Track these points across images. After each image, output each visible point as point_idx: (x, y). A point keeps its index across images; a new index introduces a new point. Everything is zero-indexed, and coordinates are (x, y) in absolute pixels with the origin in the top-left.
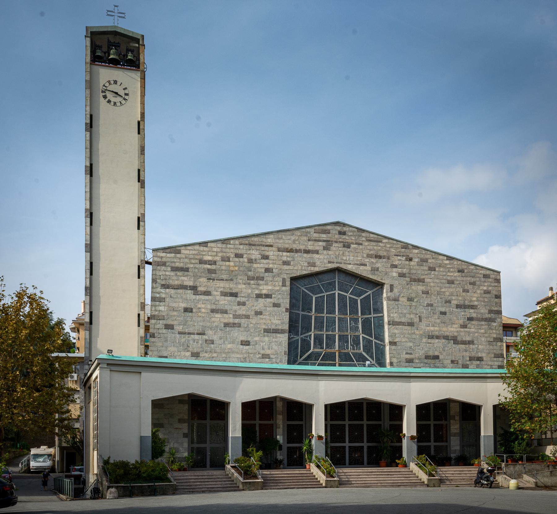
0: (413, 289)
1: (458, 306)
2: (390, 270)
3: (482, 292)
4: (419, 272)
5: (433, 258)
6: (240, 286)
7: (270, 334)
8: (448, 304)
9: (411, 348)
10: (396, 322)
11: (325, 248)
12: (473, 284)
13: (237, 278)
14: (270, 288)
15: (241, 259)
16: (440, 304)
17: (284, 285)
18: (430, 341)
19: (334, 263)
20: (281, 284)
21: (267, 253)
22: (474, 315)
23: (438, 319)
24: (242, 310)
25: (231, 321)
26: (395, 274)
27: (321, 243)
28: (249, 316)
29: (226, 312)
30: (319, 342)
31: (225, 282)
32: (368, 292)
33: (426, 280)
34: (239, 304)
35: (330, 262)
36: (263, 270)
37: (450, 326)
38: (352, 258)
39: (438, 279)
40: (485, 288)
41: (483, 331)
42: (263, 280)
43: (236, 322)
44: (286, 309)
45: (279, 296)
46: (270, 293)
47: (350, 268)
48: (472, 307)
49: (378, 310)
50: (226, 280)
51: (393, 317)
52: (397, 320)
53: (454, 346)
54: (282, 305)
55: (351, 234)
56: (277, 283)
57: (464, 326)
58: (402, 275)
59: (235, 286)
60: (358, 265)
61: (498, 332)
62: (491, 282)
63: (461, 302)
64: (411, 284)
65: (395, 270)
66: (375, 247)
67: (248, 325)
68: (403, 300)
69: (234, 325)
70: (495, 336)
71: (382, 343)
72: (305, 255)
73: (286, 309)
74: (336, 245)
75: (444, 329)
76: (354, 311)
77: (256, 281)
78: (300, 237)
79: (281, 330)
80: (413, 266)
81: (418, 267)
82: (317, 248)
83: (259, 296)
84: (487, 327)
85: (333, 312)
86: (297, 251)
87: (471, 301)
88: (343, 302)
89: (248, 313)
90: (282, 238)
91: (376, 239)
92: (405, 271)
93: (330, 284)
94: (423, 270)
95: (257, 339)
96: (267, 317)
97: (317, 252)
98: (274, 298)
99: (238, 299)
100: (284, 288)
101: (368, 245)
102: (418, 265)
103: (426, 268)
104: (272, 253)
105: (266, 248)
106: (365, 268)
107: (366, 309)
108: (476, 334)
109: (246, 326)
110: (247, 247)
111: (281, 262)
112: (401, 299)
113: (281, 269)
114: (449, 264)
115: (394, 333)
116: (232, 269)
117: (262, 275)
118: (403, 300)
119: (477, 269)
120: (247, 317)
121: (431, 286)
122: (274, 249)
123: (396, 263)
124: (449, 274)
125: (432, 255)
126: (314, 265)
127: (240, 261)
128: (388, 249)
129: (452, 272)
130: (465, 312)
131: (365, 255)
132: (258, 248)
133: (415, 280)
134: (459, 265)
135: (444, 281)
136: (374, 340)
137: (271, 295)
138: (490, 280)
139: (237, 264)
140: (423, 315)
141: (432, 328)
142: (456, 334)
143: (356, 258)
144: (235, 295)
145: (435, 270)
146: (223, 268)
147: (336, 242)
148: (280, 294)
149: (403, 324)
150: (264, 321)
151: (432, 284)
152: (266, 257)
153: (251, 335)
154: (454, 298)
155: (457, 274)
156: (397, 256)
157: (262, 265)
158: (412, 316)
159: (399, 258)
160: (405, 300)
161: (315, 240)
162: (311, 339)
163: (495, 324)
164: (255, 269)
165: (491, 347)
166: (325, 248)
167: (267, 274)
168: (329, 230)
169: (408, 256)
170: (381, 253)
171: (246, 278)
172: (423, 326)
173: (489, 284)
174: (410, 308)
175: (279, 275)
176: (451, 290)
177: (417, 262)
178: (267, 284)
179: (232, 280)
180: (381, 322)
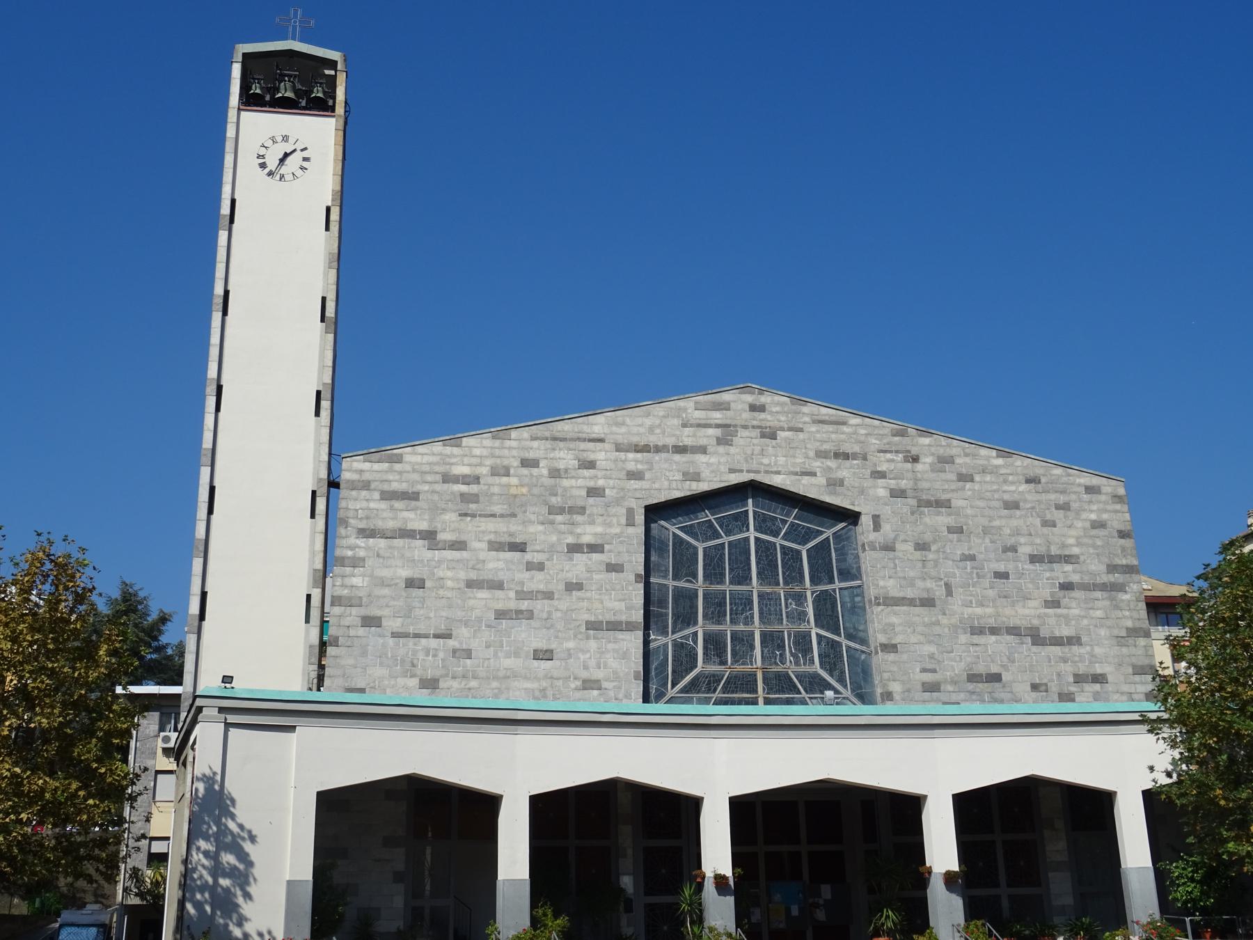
1: (1034, 559)
3: (1088, 525)
4: (938, 485)
5: (966, 455)
6: (532, 529)
8: (1009, 554)
9: (931, 656)
11: (720, 441)
12: (1065, 507)
13: (525, 512)
14: (599, 529)
15: (535, 471)
16: (992, 556)
17: (630, 523)
18: (976, 639)
19: (742, 471)
20: (623, 521)
21: (592, 457)
22: (1075, 578)
24: (537, 581)
25: (512, 605)
26: (882, 492)
27: (711, 431)
29: (499, 586)
30: (716, 649)
32: (822, 533)
33: (954, 503)
34: (530, 566)
35: (732, 471)
36: (584, 493)
38: (782, 460)
40: (1093, 516)
41: (1099, 613)
44: (638, 576)
46: (599, 542)
47: (777, 481)
48: (1068, 559)
49: (849, 573)
50: (502, 516)
53: (1034, 649)
55: (778, 409)
56: (615, 520)
57: (1054, 604)
58: (897, 494)
59: (520, 528)
60: (796, 474)
61: (1135, 615)
62: (1105, 503)
64: (922, 513)
65: (881, 482)
66: (833, 436)
67: (549, 613)
68: (905, 548)
70: (1129, 624)
71: (864, 648)
72: (677, 457)
73: (638, 576)
74: (746, 433)
75: (1008, 611)
76: (794, 575)
77: (568, 517)
79: (628, 623)
81: (933, 475)
82: (703, 442)
83: (575, 548)
84: (1107, 603)
85: (746, 579)
86: (658, 449)
87: (1064, 546)
88: (767, 556)
89: (551, 587)
90: (623, 424)
91: (833, 419)
92: (904, 484)
93: (736, 517)
94: (947, 481)
95: (571, 644)
96: (594, 595)
97: (703, 450)
98: (610, 551)
99: (528, 556)
100: (631, 530)
101: (818, 431)
104: (601, 455)
105: (591, 445)
106: (813, 480)
107: (821, 571)
108: (1085, 622)
109: (545, 615)
110: (548, 444)
111: (623, 475)
113: (623, 489)
116: (513, 491)
117: (580, 503)
118: (904, 548)
119: (1069, 475)
120: (549, 595)
121: (967, 516)
122: (606, 446)
123: (883, 467)
124: (1006, 488)
125: (964, 449)
126: (696, 477)
127: (531, 475)
128: (862, 438)
129: (1013, 483)
131: (812, 454)
132: (572, 445)
133: (929, 504)
136: (845, 643)
137: (602, 546)
138: (1103, 498)
139: (526, 480)
141: (979, 611)
142: (1036, 622)
143: (792, 460)
144: (519, 547)
145: (972, 480)
146: (496, 490)
147: (745, 427)
148: (621, 542)
149: (911, 602)
150: (585, 604)
151: (969, 511)
152: (591, 465)
154: (1022, 540)
155: (1023, 487)
157: (580, 482)
158: (929, 584)
159: (889, 456)
160: (909, 547)
161: (699, 426)
162: (695, 642)
163: (1126, 597)
164: (565, 489)
165: (1125, 650)
166: (720, 441)
167: (591, 500)
168: (729, 403)
169: (909, 451)
170: (847, 448)
171: (545, 510)
173: (1101, 506)
174: (924, 567)
175: (618, 501)
176: (1014, 523)
177: (931, 465)
178: (592, 523)
179: (514, 515)
180: (857, 599)
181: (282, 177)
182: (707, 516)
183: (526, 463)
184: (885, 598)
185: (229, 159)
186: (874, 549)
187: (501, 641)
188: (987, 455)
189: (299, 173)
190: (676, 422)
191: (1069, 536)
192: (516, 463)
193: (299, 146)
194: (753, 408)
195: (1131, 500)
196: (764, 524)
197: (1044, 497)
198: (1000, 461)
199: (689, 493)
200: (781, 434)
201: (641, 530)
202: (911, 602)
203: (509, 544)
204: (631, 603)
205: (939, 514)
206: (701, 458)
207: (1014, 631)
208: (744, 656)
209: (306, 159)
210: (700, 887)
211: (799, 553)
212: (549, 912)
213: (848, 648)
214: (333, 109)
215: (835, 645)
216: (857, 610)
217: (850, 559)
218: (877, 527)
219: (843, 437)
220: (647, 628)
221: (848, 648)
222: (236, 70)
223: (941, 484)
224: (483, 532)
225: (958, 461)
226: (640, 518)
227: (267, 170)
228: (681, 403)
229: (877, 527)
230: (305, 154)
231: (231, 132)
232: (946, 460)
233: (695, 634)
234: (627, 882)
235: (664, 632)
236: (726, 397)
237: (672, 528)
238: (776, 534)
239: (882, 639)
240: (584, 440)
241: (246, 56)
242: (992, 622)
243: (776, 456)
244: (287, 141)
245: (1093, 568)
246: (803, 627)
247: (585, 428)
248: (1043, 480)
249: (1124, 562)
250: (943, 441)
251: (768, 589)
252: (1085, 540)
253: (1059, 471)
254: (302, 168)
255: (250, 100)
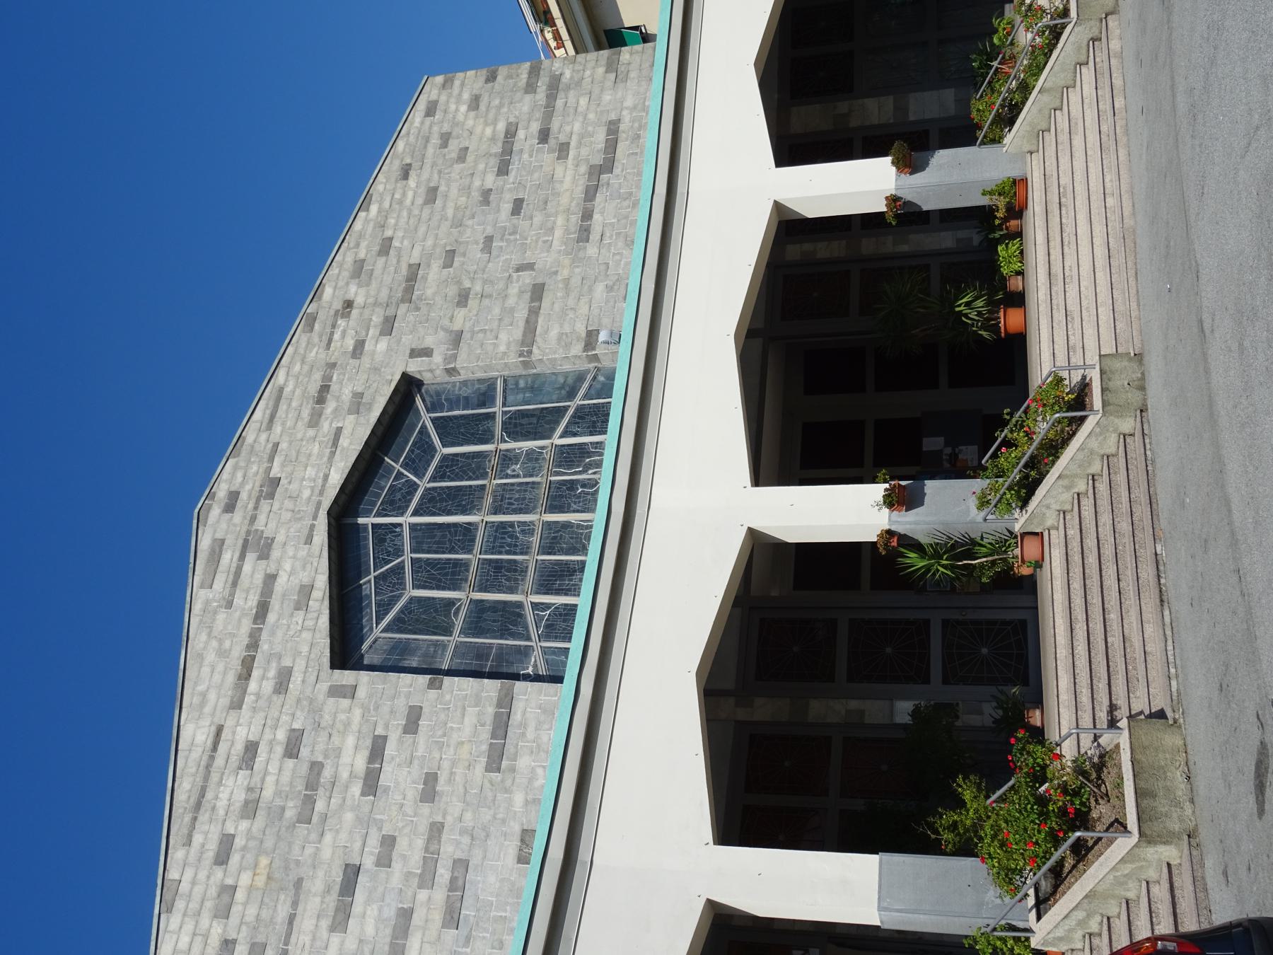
0: (435, 294)
1: (503, 170)
2: (366, 361)
3: (472, 114)
4: (388, 279)
5: (358, 245)
6: (326, 853)
7: (509, 749)
8: (492, 198)
9: (609, 289)
10: (525, 334)
11: (264, 555)
12: (445, 139)
13: (298, 863)
14: (350, 741)
15: (239, 842)
16: (490, 218)
17: (350, 692)
18: (595, 236)
19: (312, 526)
20: (345, 703)
21: (239, 747)
22: (535, 127)
23: (531, 218)
24: (410, 851)
25: (439, 895)
26: (383, 345)
27: (247, 568)
28: (433, 824)
29: (406, 915)
30: (561, 577)
31: (300, 908)
32: (424, 430)
33: (414, 260)
34: (384, 861)
35: (309, 540)
36: (290, 763)
37: (557, 186)
38: (310, 472)
39: (416, 229)
40: (463, 108)
41: (583, 101)
42: (321, 765)
43: (447, 876)
44: (431, 685)
45: (385, 709)
46: (369, 742)
47: (337, 478)
48: (510, 134)
49: (484, 394)
50: (295, 904)
51: (509, 344)
52: (518, 333)
53: (617, 171)
54: (414, 702)
55: (239, 475)
56: (342, 717)
57: (563, 149)
58: (388, 327)
59: (320, 873)
60: (333, 453)
61: (592, 64)
62: (450, 96)
63: (491, 164)
64: (420, 299)
65: (368, 346)
66: (294, 404)
67: (463, 832)
68: (461, 319)
69: (457, 886)
70: (601, 70)
71: (589, 377)
72: (271, 617)
73: (431, 685)
74: (262, 518)
75: (565, 200)
76: (474, 466)
77: (321, 791)
78: (215, 633)
79: (499, 705)
80: (367, 296)
81: (374, 285)
82: (259, 578)
83: (371, 783)
84: (572, 93)
85: (469, 529)
86: (254, 644)
87: (493, 139)
88: (442, 500)
89: (423, 827)
90: (204, 695)
91: (271, 403)
92: (377, 319)
93: (379, 541)
94: (385, 268)
95: (519, 798)
96: (449, 754)
97: (271, 579)
98: (387, 727)
99: (368, 862)
100: (361, 693)
101: (283, 424)
102: (368, 285)
103: (381, 261)
104: (240, 732)
105: (223, 747)
106: (346, 432)
107: (476, 429)
108: (591, 116)
109: (466, 840)
110: (203, 817)
111: (278, 700)
112: (457, 326)
113: (299, 701)
114: (381, 203)
115: (559, 339)
116: (261, 881)
117: (304, 769)
118: (461, 319)
119: (408, 134)
120: (436, 830)
121: (435, 245)
122: (229, 723)
123: (350, 343)
124: (408, 202)
125: (349, 248)
126: (306, 591)
127: (244, 848)
128: (306, 368)
129: (404, 194)
130: (522, 151)
131: (311, 432)
132: (215, 777)
133: (409, 290)
134: (388, 179)
135: (427, 211)
136: (578, 401)
137: (376, 738)
138: (443, 98)
139: (250, 857)
140: (516, 259)
141: (558, 233)
142: (583, 169)
143: (313, 458)
144: (352, 873)
145: (391, 239)
146: (252, 911)
147: (253, 519)
148: (377, 708)
149: (534, 312)
150: (459, 771)
151: (430, 242)
152: (251, 749)
153: (504, 821)
154: (477, 183)
155: (412, 182)
156: (330, 341)
157: (273, 769)
158: (514, 290)
159: (337, 336)
160: (461, 314)
161: (235, 584)
162: (548, 606)
163: (568, 74)
164: (278, 793)
165: (632, 75)
166: (264, 555)
167: (304, 752)
168: (215, 540)
169: (337, 312)
170: (313, 389)
171: (302, 829)
172: (544, 259)
173: (453, 100)
174: (490, 296)
175: (315, 710)
176: (454, 192)
177: (360, 286)
178: (338, 752)
179: (299, 883)
180: (522, 384)
182: (368, 582)
183: (222, 859)
184: (523, 343)
186: (455, 357)
187: (498, 919)
188: (363, 223)
190: (221, 616)
191: (482, 133)
192: (219, 873)
194: (230, 508)
195: (450, 66)
196: (396, 504)
197: (428, 161)
198: (374, 208)
199: (327, 602)
200: (275, 472)
201: (364, 677)
202: (534, 312)
203: (342, 894)
204: (471, 698)
205: (425, 278)
206: (282, 581)
207: (590, 194)
208: (578, 537)
210: (908, 542)
211: (445, 458)
212: (949, 817)
213: (586, 397)
215: (580, 414)
216: (535, 386)
217: (466, 392)
218: (427, 352)
219: (298, 392)
220: (516, 677)
221: (586, 397)
223: (387, 275)
224: (314, 939)
225: (362, 255)
226: (346, 677)
228: (197, 607)
229: (427, 352)
232: (359, 269)
233: (535, 606)
234: (903, 710)
235: (525, 652)
236: (205, 543)
237: (377, 634)
238: (414, 487)
239: (577, 349)
240: (212, 758)
242: (575, 219)
243: (303, 479)
245: (526, 109)
246: (548, 455)
247: (195, 754)
248: (408, 161)
249: (524, 76)
250: (334, 271)
251: (488, 500)
252: (491, 115)
253: (400, 145)
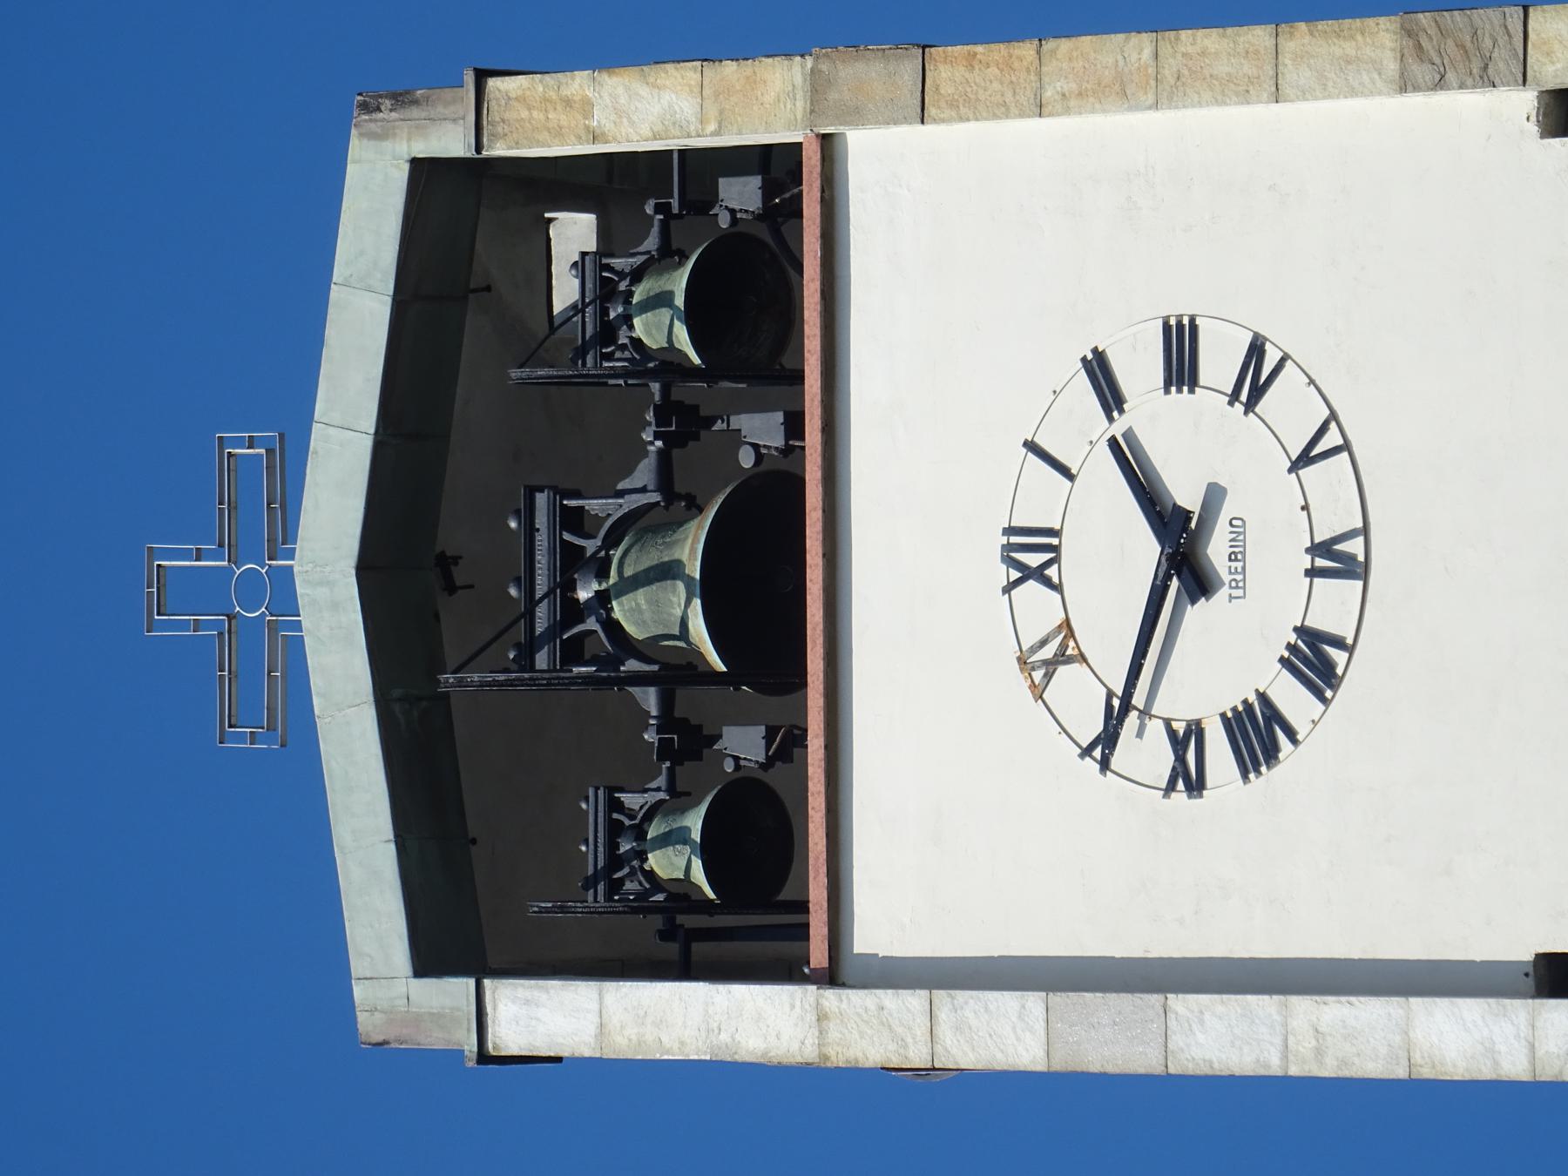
181: (1334, 560)
185: (1220, 1038)
189: (1291, 409)
193: (1080, 427)
209: (1181, 360)
214: (776, 166)
222: (545, 1016)
227: (1292, 698)
230: (1141, 369)
231: (1003, 1035)
241: (434, 953)
244: (1047, 540)
254: (1253, 382)
255: (760, 895)
